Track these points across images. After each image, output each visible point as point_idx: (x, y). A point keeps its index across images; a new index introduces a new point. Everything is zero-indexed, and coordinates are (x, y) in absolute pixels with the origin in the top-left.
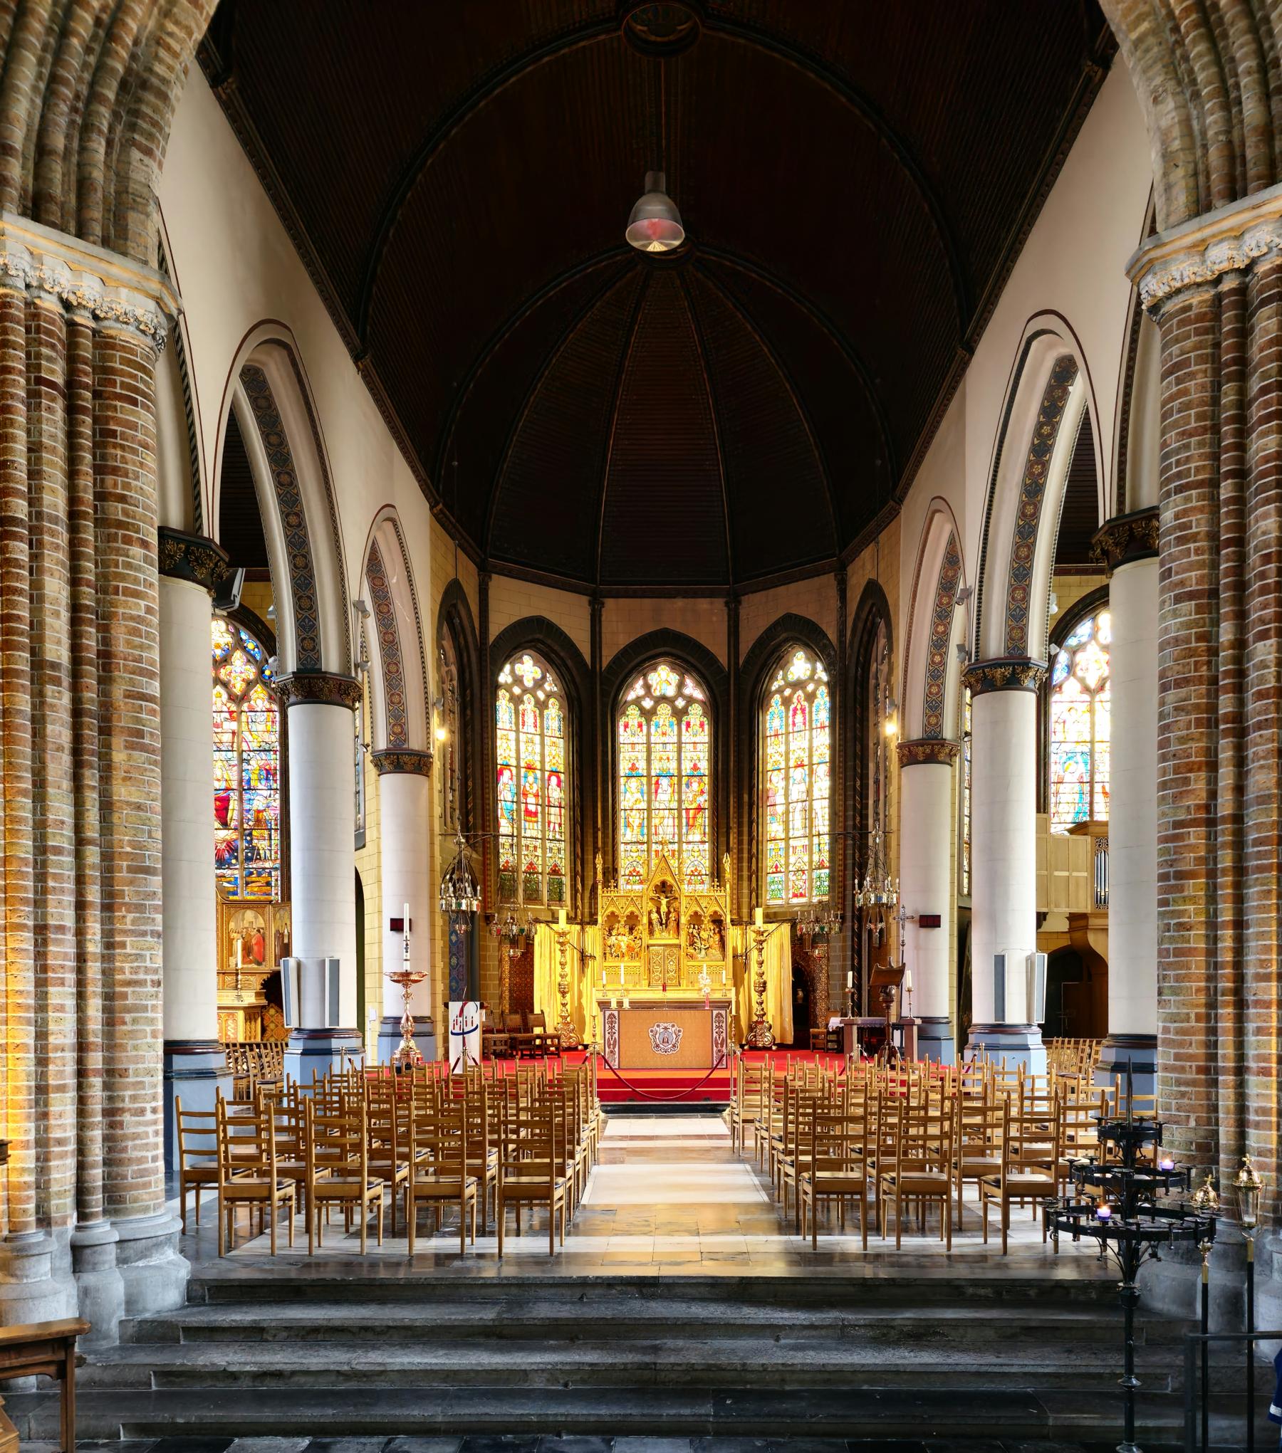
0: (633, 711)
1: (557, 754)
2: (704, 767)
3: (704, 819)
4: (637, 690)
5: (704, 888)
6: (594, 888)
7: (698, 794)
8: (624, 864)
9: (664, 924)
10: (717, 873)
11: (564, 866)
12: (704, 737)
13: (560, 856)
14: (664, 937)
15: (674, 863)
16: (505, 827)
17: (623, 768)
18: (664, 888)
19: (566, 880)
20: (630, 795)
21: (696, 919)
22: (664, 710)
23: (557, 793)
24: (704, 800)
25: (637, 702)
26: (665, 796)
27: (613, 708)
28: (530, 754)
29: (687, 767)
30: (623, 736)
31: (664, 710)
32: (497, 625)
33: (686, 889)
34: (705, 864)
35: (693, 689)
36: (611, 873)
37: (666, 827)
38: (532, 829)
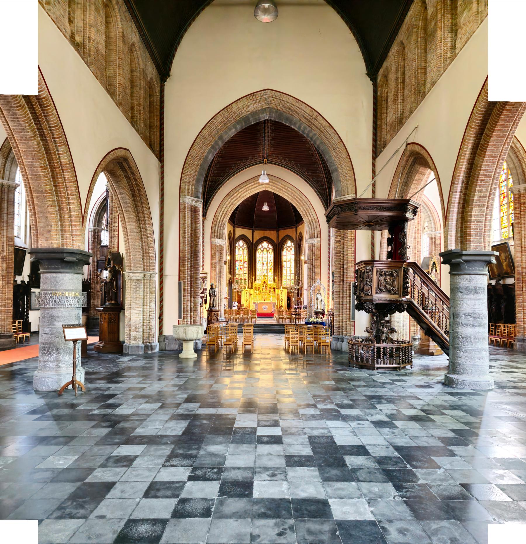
0: (259, 250)
1: (246, 258)
2: (272, 261)
3: (272, 270)
4: (260, 247)
5: (272, 282)
6: (252, 282)
7: (271, 265)
8: (257, 278)
9: (265, 289)
10: (274, 280)
11: (247, 278)
12: (272, 255)
13: (246, 276)
14: (264, 291)
15: (266, 278)
16: (237, 271)
17: (257, 260)
18: (265, 282)
19: (247, 281)
20: (259, 265)
21: (270, 288)
22: (265, 250)
23: (246, 265)
24: (272, 266)
25: (260, 249)
26: (265, 266)
27: (256, 249)
28: (241, 258)
29: (269, 261)
30: (258, 255)
31: (265, 250)
32: (236, 236)
33: (269, 283)
34: (272, 278)
35: (270, 246)
36: (255, 279)
37: (265, 271)
38: (241, 272)
